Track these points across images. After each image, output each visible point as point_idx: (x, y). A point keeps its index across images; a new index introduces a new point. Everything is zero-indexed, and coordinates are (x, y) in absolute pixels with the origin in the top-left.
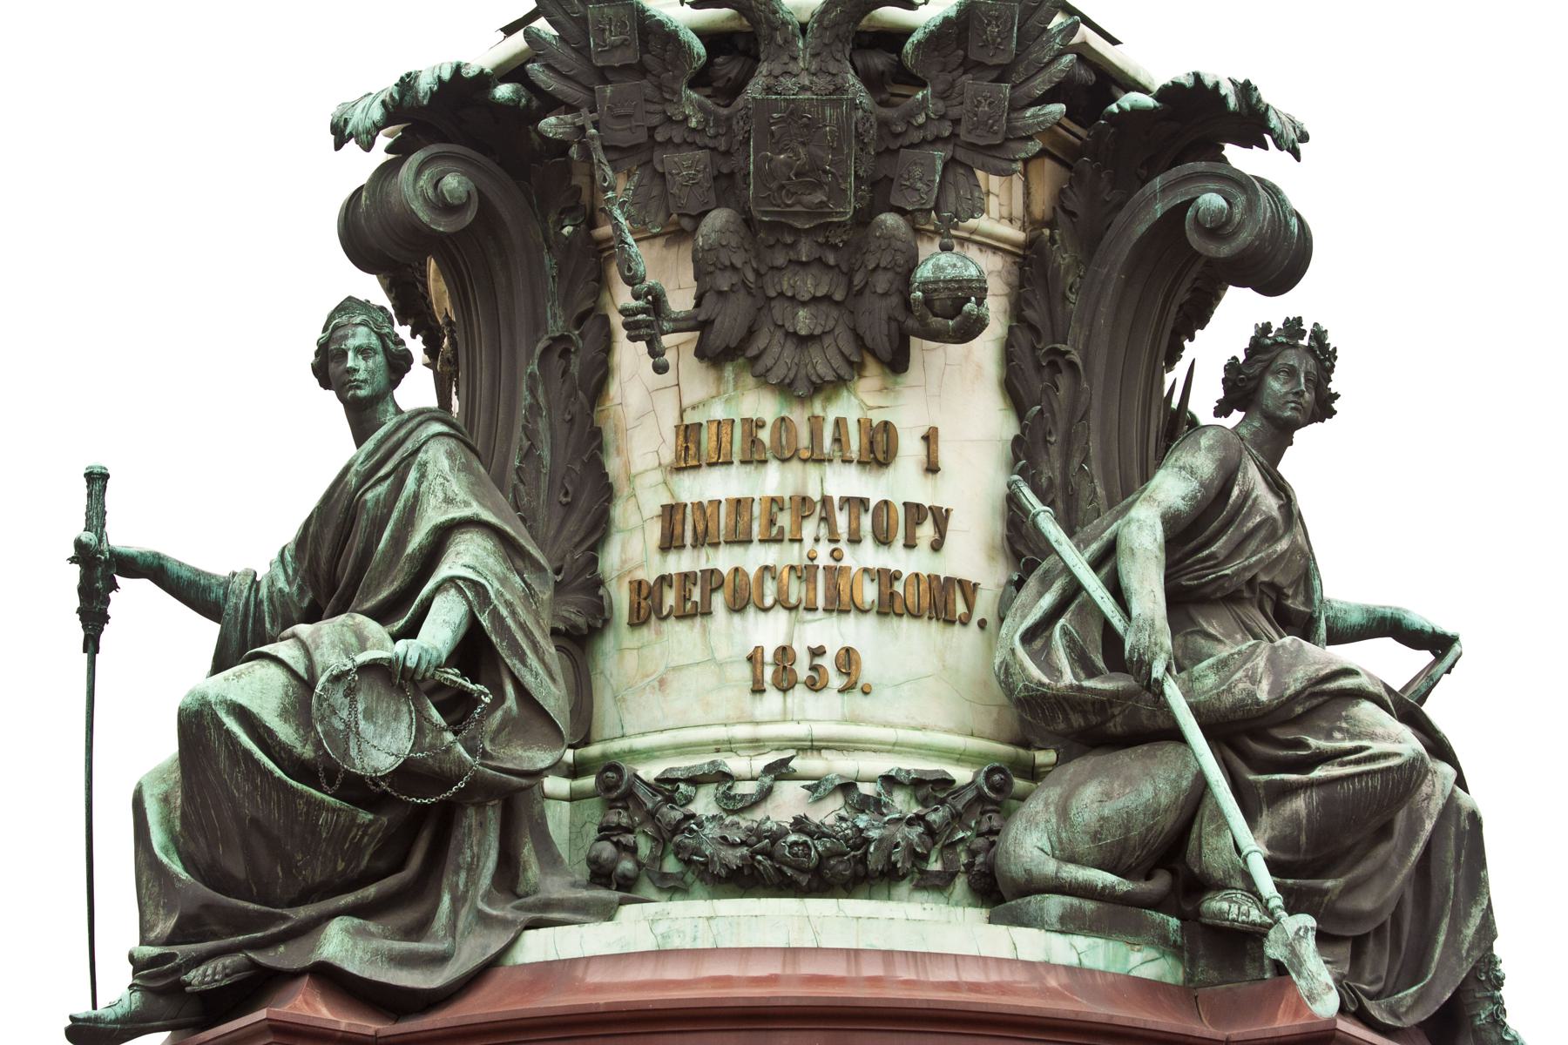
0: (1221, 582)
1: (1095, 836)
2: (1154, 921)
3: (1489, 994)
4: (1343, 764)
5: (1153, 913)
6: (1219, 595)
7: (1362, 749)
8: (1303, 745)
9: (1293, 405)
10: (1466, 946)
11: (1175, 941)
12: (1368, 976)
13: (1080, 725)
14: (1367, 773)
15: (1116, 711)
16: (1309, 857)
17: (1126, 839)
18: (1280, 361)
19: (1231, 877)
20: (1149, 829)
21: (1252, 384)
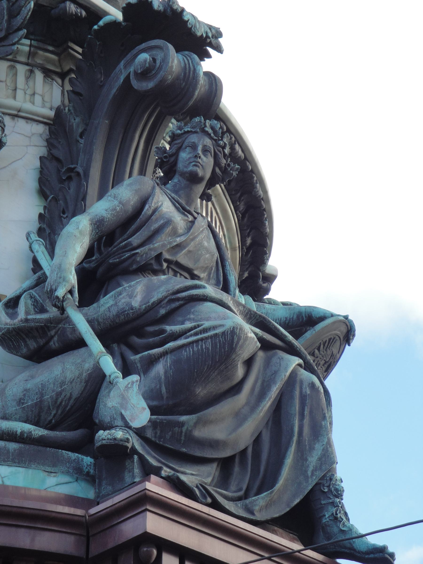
0: (134, 258)
1: (20, 402)
2: (69, 458)
3: (331, 501)
4: (186, 338)
5: (70, 453)
6: (134, 267)
7: (199, 326)
8: (163, 331)
9: (193, 163)
10: (311, 468)
11: (88, 473)
12: (233, 487)
13: (34, 347)
14: (202, 340)
15: (53, 332)
16: (171, 403)
17: (41, 401)
18: (187, 141)
19: (115, 419)
20: (59, 394)
21: (172, 159)
